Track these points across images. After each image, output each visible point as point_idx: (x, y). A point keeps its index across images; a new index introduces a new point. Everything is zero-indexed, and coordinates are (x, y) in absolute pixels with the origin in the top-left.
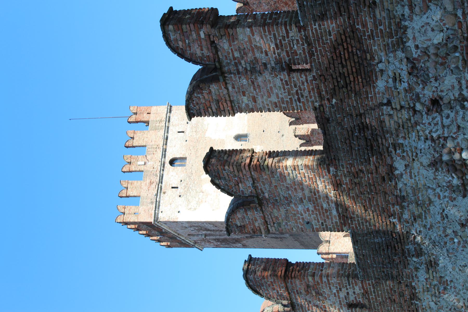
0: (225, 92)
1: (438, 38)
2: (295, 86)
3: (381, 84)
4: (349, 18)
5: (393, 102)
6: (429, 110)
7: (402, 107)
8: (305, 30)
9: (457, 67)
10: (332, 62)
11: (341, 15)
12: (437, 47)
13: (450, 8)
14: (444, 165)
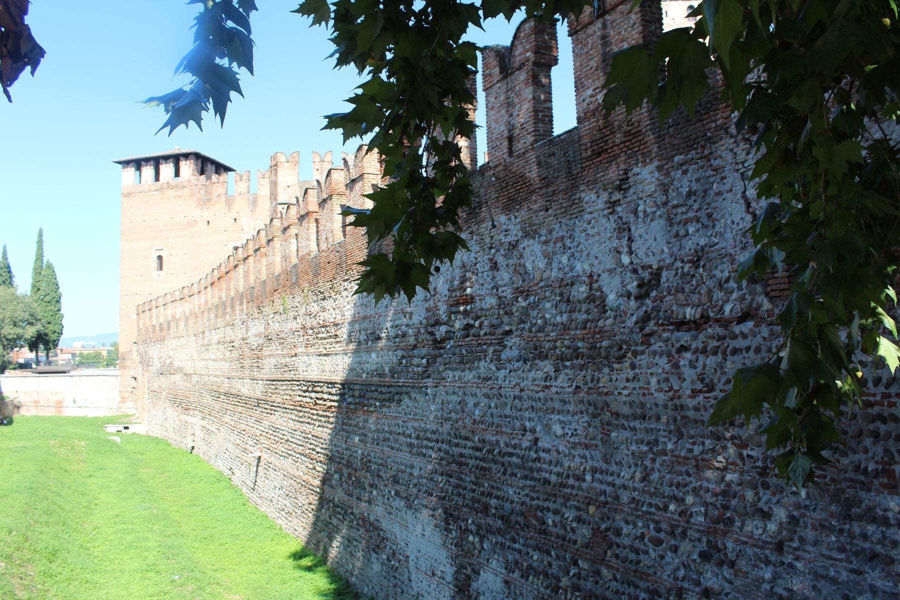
0: (495, 81)
1: (529, 266)
2: (501, 144)
3: (503, 218)
4: (539, 188)
5: (495, 229)
6: (491, 260)
7: (492, 237)
8: (532, 149)
9: (513, 283)
10: (515, 174)
11: (541, 181)
12: (524, 266)
13: (545, 276)
14: (464, 273)
